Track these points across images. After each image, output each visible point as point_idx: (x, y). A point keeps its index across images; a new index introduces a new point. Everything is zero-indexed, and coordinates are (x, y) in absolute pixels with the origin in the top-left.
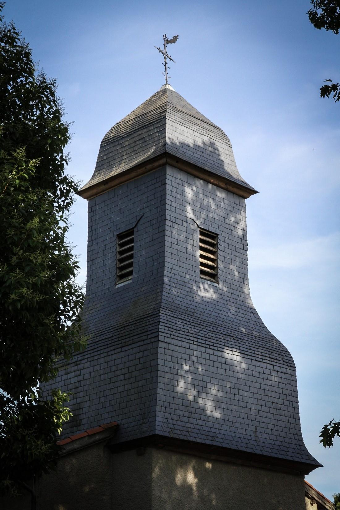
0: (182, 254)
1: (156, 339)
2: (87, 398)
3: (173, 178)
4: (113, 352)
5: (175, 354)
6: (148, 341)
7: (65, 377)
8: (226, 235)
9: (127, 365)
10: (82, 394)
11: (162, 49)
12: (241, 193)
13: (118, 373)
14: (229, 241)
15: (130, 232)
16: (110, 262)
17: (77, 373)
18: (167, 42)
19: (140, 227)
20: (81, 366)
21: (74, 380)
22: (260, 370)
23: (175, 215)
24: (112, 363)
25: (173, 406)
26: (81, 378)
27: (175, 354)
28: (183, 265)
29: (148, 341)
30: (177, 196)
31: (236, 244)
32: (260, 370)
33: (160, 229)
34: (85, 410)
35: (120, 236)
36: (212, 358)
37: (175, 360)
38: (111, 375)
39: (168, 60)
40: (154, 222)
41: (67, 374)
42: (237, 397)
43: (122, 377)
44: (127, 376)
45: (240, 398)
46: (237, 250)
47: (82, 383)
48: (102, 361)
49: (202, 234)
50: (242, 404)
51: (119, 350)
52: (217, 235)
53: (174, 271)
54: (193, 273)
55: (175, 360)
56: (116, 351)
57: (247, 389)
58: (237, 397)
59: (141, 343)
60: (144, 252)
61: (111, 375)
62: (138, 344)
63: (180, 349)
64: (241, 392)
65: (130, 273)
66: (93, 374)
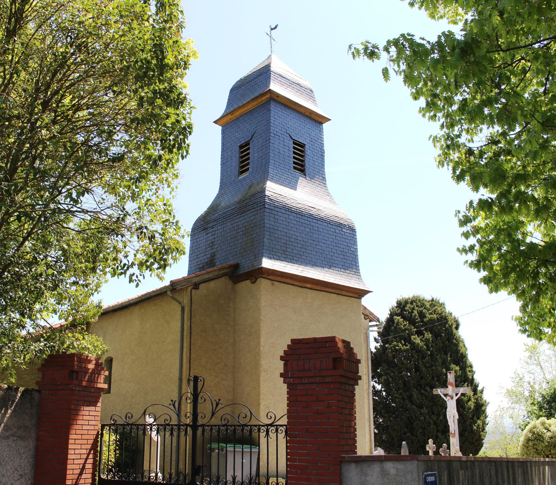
0: (281, 155)
1: (263, 206)
2: (219, 249)
3: (273, 107)
4: (235, 218)
5: (276, 217)
6: (259, 208)
7: (206, 236)
8: (311, 146)
9: (245, 225)
10: (216, 246)
11: (269, 33)
12: (320, 120)
13: (238, 231)
14: (313, 150)
15: (247, 144)
16: (235, 162)
17: (214, 233)
18: (272, 29)
19: (253, 139)
20: (216, 229)
21: (212, 237)
22: (333, 230)
23: (276, 130)
24: (235, 225)
25: (274, 250)
26: (215, 236)
27: (276, 217)
28: (282, 162)
29: (259, 208)
30: (278, 118)
31: (317, 152)
32: (333, 230)
33: (267, 139)
34: (218, 256)
35: (241, 147)
36: (301, 220)
37: (276, 220)
38: (234, 232)
39: (272, 40)
40: (263, 135)
41: (207, 234)
42: (318, 247)
43: (241, 233)
44: (244, 232)
45: (320, 247)
46: (318, 155)
47: (216, 239)
48: (229, 224)
49: (294, 143)
50: (321, 251)
51: (239, 216)
52: (305, 145)
53: (276, 166)
54: (289, 168)
55: (276, 220)
56: (237, 217)
57: (325, 242)
58: (318, 247)
59: (253, 210)
60: (256, 154)
61: (234, 232)
62: (251, 211)
63: (279, 214)
64: (321, 244)
65: (248, 169)
66: (223, 233)
